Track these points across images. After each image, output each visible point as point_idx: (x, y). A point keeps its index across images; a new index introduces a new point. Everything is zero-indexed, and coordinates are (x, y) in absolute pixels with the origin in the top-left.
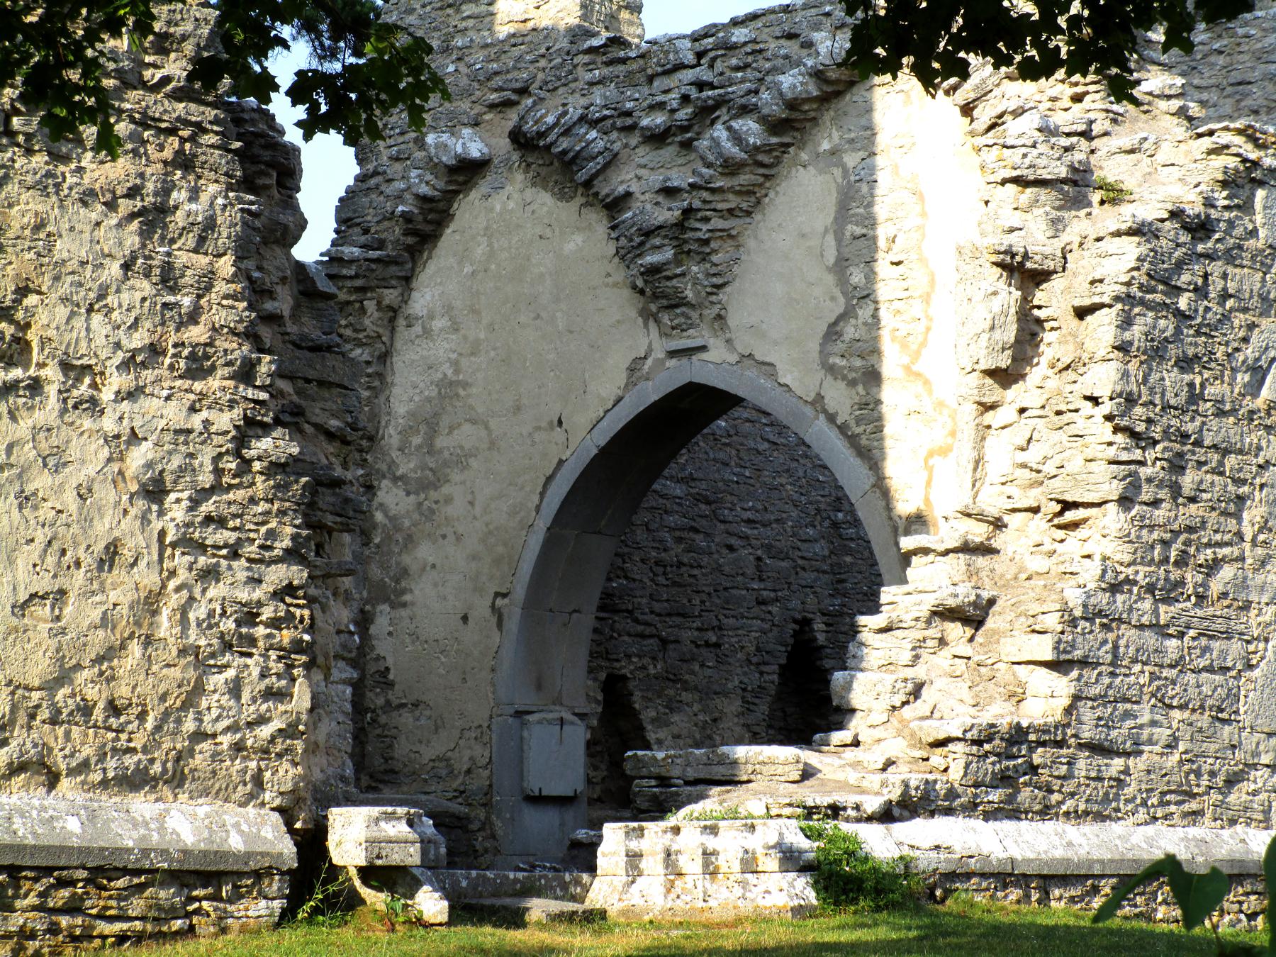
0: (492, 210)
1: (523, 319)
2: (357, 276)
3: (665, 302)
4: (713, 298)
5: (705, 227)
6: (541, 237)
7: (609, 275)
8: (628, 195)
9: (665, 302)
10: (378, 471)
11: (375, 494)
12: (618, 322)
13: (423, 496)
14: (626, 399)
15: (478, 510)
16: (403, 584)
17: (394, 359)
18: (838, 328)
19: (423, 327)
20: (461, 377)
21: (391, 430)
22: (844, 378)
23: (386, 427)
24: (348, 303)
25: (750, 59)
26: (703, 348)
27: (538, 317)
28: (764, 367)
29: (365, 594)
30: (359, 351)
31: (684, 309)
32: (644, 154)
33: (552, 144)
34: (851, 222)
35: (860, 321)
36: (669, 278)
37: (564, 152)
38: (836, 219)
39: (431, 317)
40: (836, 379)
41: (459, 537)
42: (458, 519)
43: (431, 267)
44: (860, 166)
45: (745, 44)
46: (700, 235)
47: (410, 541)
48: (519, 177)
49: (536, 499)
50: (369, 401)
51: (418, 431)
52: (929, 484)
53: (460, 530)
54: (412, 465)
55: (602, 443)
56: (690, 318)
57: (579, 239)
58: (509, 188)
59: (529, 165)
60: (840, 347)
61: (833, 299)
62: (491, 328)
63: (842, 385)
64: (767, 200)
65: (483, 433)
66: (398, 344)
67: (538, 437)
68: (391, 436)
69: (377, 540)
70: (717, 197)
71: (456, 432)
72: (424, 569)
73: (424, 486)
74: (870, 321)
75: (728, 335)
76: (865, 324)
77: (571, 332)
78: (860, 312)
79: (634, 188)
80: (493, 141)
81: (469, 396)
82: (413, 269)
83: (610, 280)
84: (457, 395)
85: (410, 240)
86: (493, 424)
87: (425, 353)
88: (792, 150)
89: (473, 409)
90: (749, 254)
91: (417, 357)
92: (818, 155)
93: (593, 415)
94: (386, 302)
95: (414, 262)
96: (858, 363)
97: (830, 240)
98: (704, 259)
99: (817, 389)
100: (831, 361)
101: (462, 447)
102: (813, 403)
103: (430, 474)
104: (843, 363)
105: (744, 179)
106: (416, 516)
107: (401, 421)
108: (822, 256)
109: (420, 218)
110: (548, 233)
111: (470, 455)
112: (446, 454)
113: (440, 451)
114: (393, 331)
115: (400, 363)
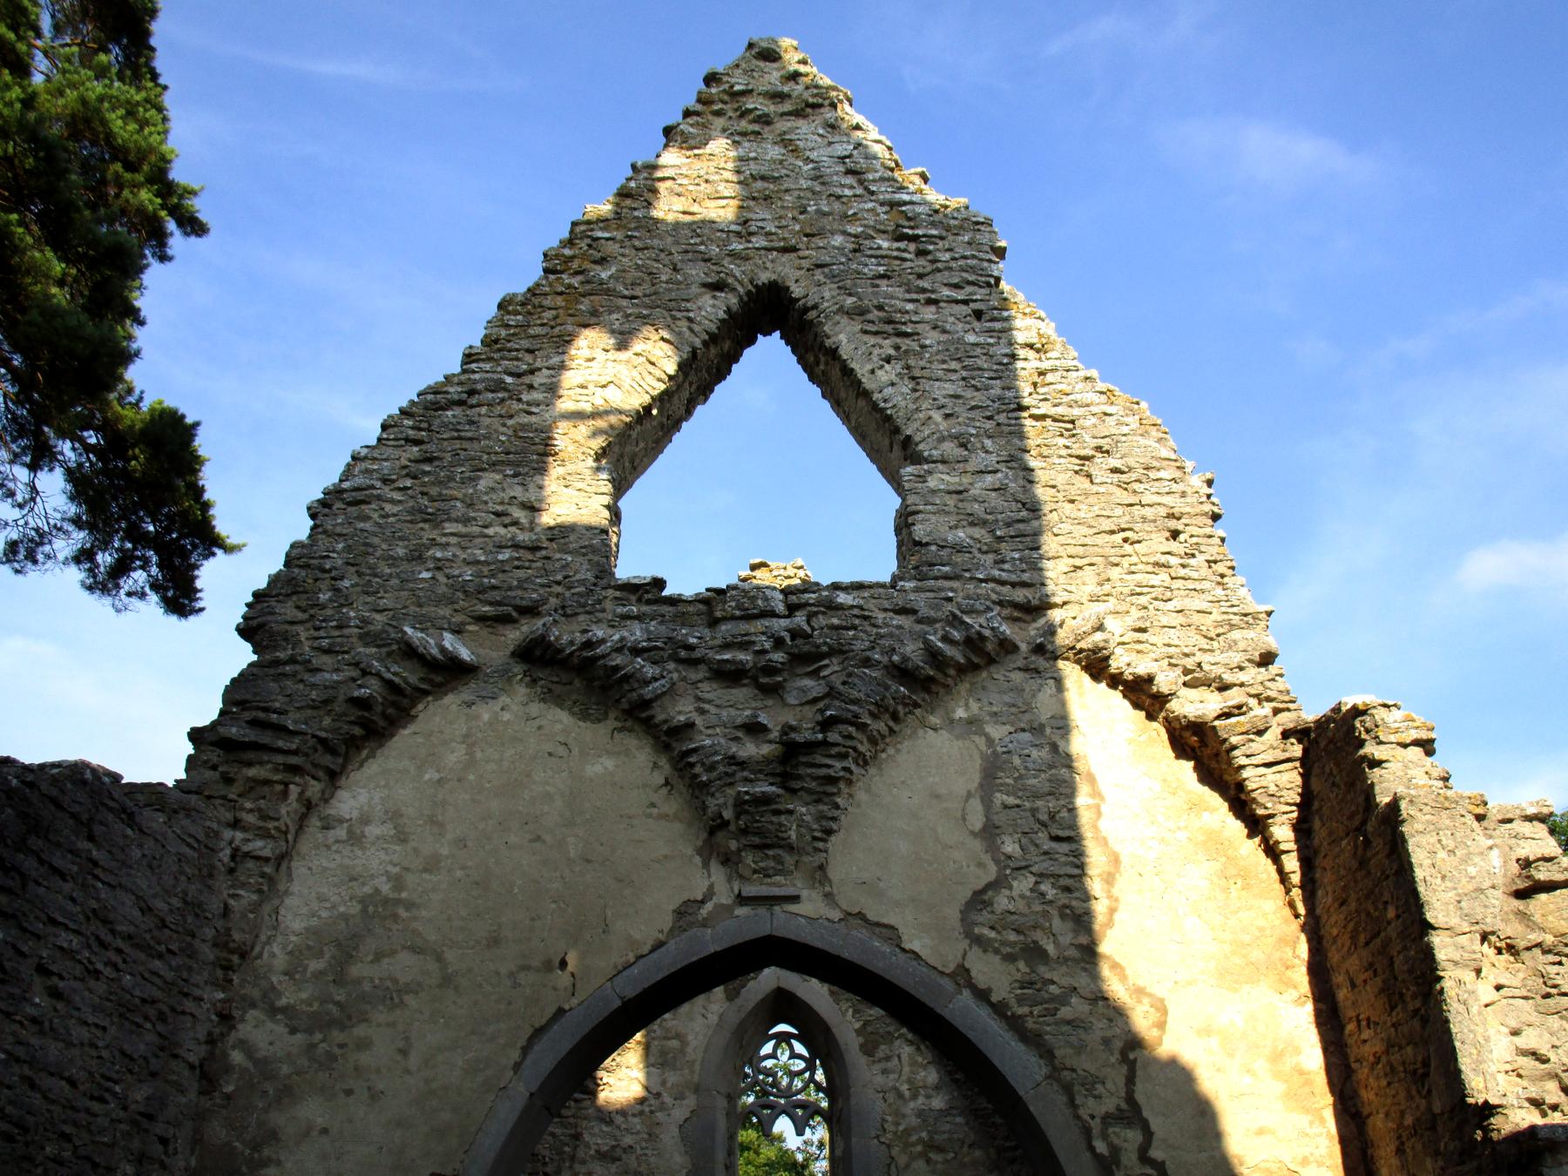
0: (477, 717)
1: (513, 839)
2: (295, 753)
3: (757, 840)
4: (820, 845)
5: (838, 765)
6: (550, 754)
7: (653, 805)
8: (690, 725)
9: (757, 840)
10: (244, 998)
11: (233, 1027)
12: (666, 857)
13: (318, 1036)
14: (671, 945)
15: (414, 1061)
16: (266, 1152)
17: (294, 864)
18: (986, 897)
19: (350, 832)
20: (404, 895)
21: (276, 949)
22: (997, 951)
23: (269, 941)
24: (267, 782)
25: (857, 622)
27: (538, 838)
28: (877, 930)
29: (193, 1162)
30: (259, 843)
31: (780, 852)
32: (710, 690)
33: (603, 656)
34: (1000, 791)
35: (1015, 893)
36: (778, 813)
37: (616, 669)
38: (981, 785)
39: (365, 820)
40: (985, 951)
41: (375, 1096)
42: (378, 1071)
43: (372, 768)
44: (1007, 739)
45: (852, 607)
46: (831, 772)
47: (287, 1094)
48: (522, 691)
49: (515, 1055)
50: (255, 907)
51: (321, 954)
52: (1130, 1080)
53: (381, 1086)
54: (304, 995)
55: (630, 993)
56: (782, 863)
57: (610, 763)
58: (504, 699)
59: (534, 681)
60: (985, 916)
61: (980, 865)
62: (462, 843)
63: (997, 959)
64: (884, 755)
65: (433, 966)
66: (304, 846)
67: (523, 978)
68: (275, 956)
69: (229, 1089)
70: (859, 736)
71: (386, 960)
72: (307, 1134)
73: (320, 1023)
74: (1028, 894)
75: (828, 889)
76: (1022, 896)
77: (588, 861)
78: (1015, 884)
79: (699, 721)
80: (481, 651)
81: (415, 919)
82: (344, 767)
83: (655, 811)
84: (395, 917)
85: (357, 731)
86: (450, 955)
87: (347, 862)
88: (918, 711)
89: (419, 934)
90: (859, 806)
91: (332, 865)
92: (952, 721)
93: (617, 959)
94: (308, 794)
95: (347, 759)
96: (1013, 937)
97: (976, 806)
98: (818, 801)
99: (959, 959)
100: (976, 930)
101: (395, 981)
102: (951, 976)
103: (334, 1009)
104: (993, 934)
105: (879, 726)
106: (303, 1062)
107: (293, 938)
108: (964, 819)
109: (379, 709)
110: (561, 750)
111: (408, 989)
112: (367, 987)
113: (358, 981)
114: (300, 829)
115: (304, 871)
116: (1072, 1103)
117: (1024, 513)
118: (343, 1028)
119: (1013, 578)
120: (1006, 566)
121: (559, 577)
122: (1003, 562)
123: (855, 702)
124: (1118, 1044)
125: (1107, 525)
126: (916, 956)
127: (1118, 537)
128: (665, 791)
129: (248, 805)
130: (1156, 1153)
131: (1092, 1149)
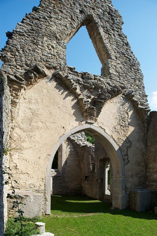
7: (75, 106)
13: (28, 133)
26: (93, 123)
52: (127, 151)
61: (115, 123)
65: (45, 125)
86: (47, 124)
116: (121, 152)
117: (123, 73)
118: (32, 132)
119: (121, 82)
120: (121, 80)
121: (59, 63)
122: (120, 79)
123: (106, 96)
124: (126, 147)
125: (133, 78)
126: (107, 133)
127: (133, 80)
128: (77, 104)
129: (14, 92)
130: (129, 159)
131: (123, 158)
